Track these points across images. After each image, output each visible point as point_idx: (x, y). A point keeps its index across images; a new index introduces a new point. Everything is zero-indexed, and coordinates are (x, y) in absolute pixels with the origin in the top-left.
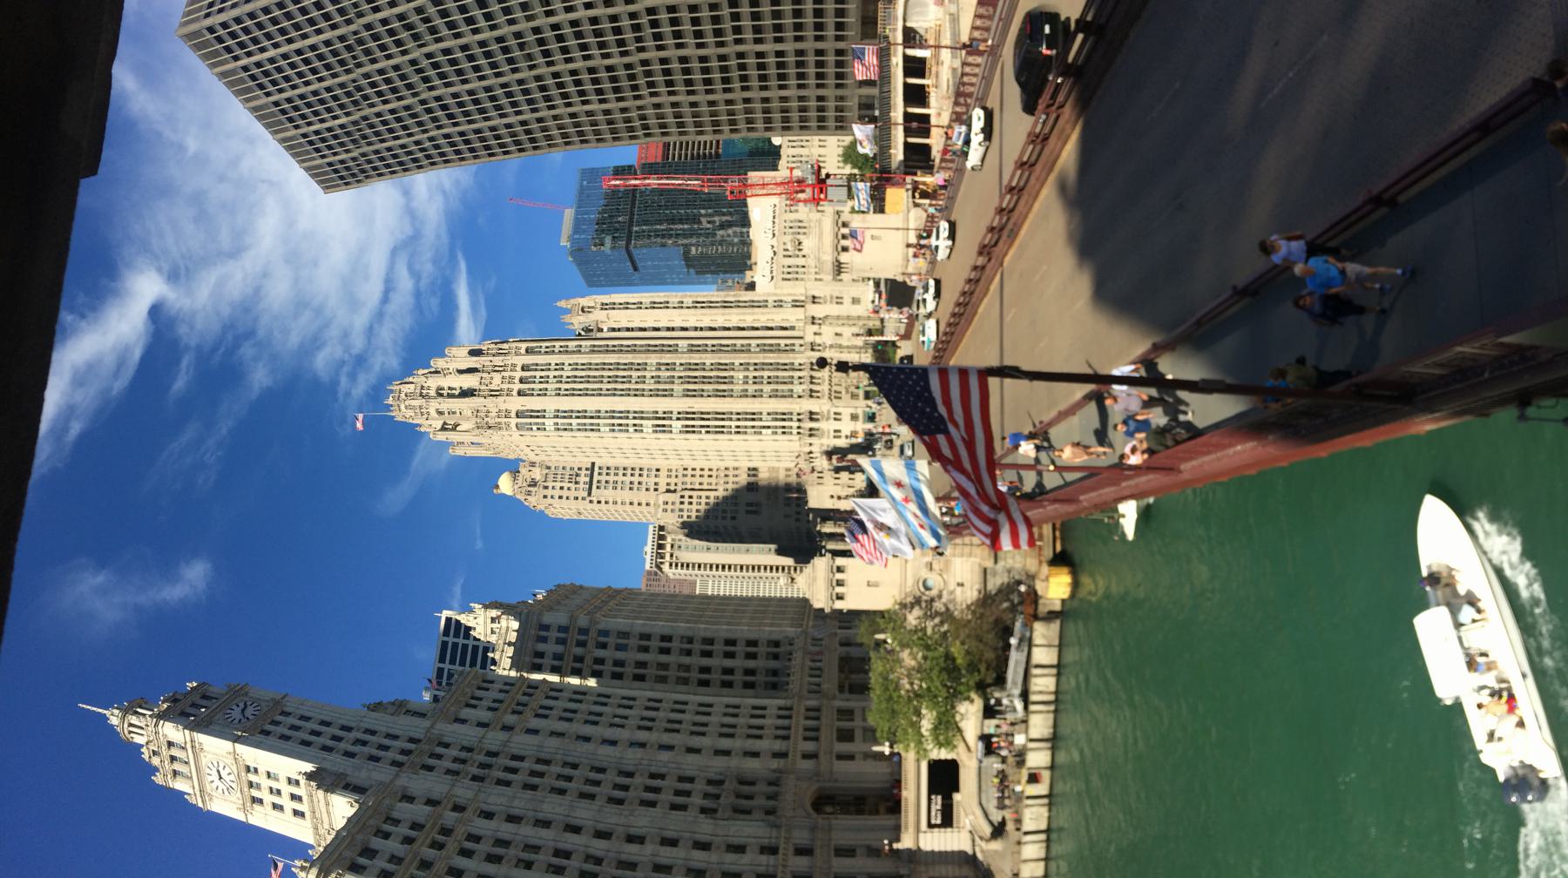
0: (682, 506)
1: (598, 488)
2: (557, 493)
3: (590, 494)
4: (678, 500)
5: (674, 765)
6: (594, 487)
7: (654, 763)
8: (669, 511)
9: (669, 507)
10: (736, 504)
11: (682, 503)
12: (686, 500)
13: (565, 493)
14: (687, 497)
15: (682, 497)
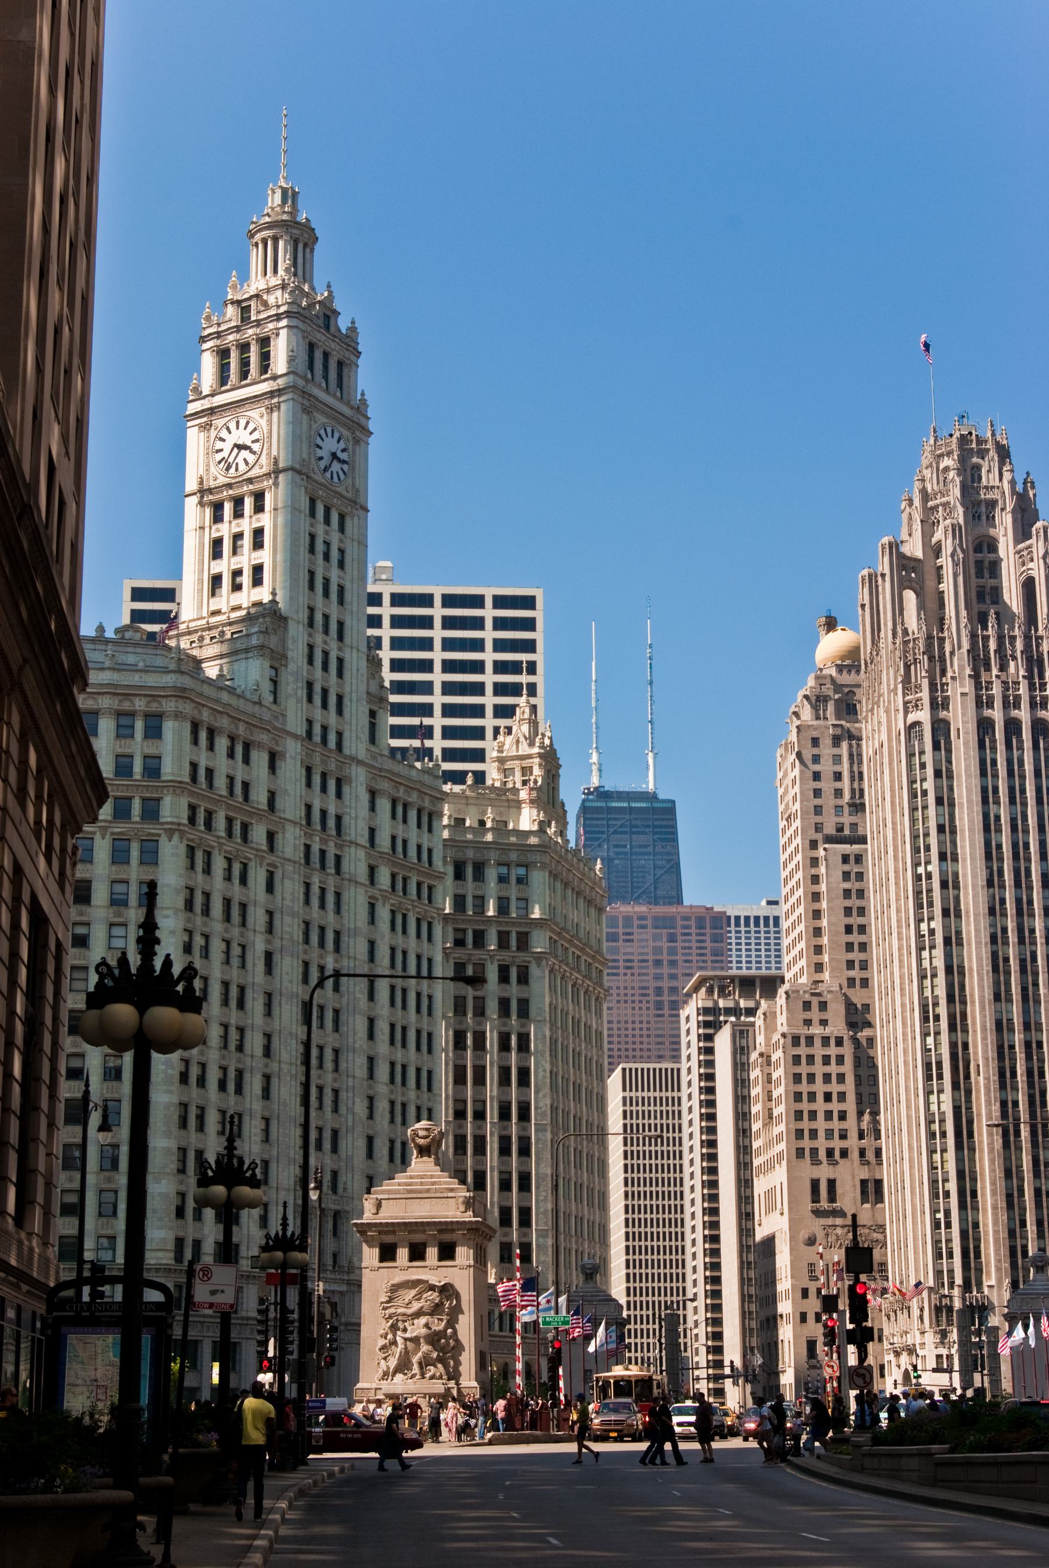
0: (818, 1042)
1: (845, 859)
2: (826, 767)
3: (829, 839)
4: (828, 1031)
5: (350, 1124)
6: (846, 848)
7: (350, 1094)
8: (807, 1015)
9: (815, 1014)
10: (830, 1153)
11: (826, 1041)
12: (833, 1051)
13: (827, 785)
14: (840, 1051)
15: (839, 1042)
